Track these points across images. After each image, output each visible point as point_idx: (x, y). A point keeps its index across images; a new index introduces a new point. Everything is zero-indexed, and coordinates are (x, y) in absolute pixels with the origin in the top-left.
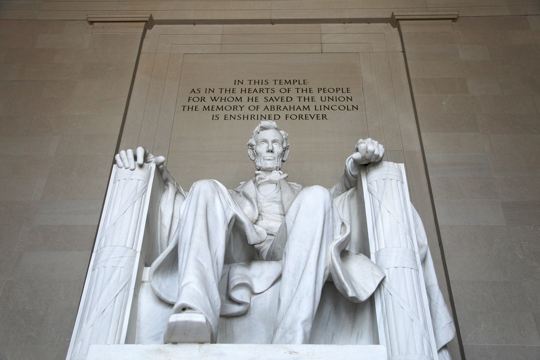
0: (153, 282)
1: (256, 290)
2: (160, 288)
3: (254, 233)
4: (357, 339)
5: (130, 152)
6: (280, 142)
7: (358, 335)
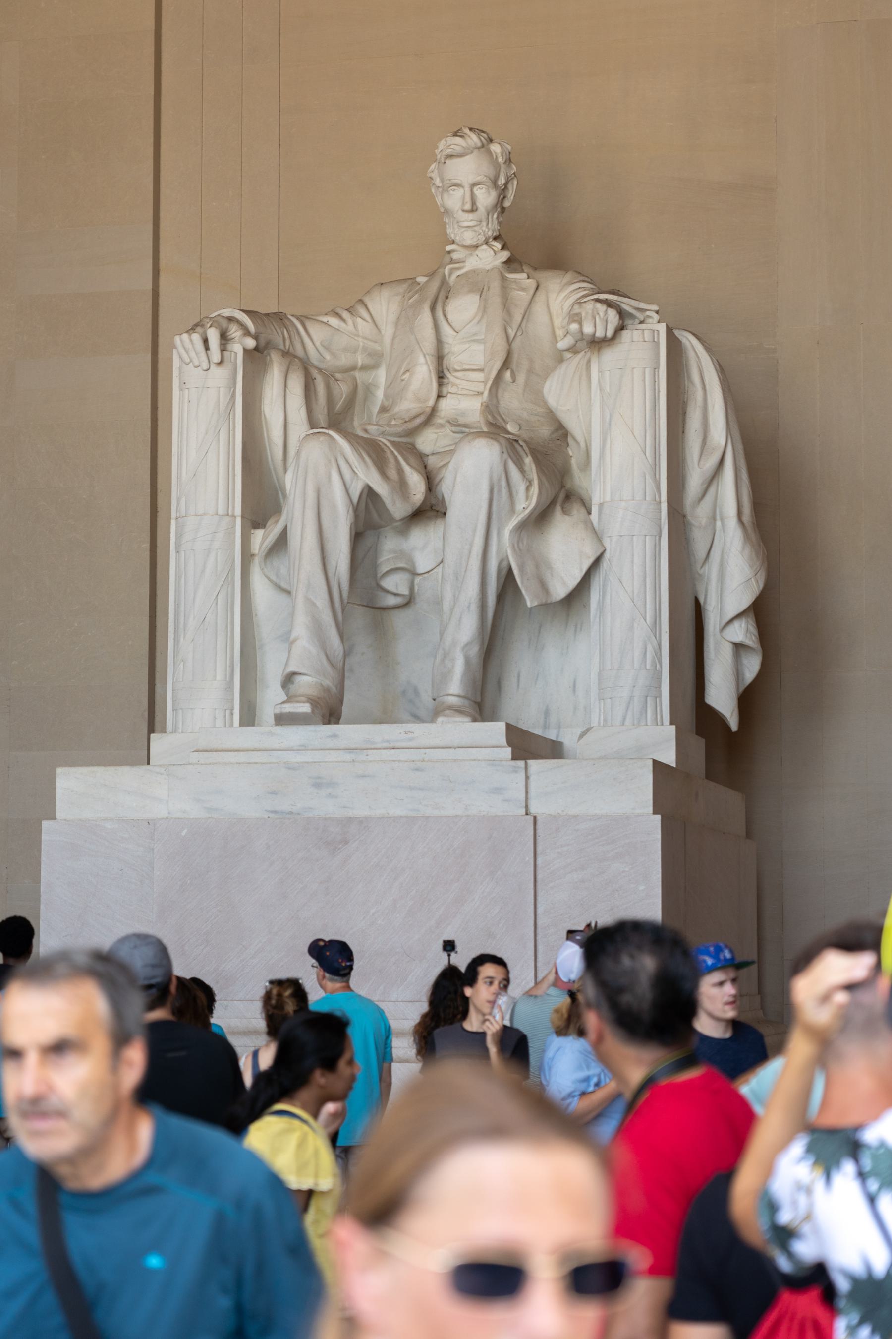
0: (265, 570)
1: (420, 571)
2: (277, 575)
3: (399, 504)
4: (576, 631)
5: (196, 337)
6: (489, 183)
7: (576, 627)
